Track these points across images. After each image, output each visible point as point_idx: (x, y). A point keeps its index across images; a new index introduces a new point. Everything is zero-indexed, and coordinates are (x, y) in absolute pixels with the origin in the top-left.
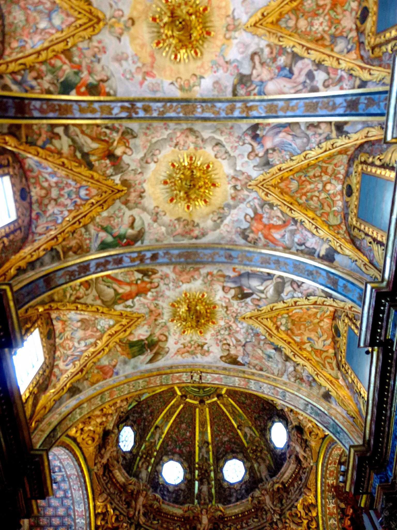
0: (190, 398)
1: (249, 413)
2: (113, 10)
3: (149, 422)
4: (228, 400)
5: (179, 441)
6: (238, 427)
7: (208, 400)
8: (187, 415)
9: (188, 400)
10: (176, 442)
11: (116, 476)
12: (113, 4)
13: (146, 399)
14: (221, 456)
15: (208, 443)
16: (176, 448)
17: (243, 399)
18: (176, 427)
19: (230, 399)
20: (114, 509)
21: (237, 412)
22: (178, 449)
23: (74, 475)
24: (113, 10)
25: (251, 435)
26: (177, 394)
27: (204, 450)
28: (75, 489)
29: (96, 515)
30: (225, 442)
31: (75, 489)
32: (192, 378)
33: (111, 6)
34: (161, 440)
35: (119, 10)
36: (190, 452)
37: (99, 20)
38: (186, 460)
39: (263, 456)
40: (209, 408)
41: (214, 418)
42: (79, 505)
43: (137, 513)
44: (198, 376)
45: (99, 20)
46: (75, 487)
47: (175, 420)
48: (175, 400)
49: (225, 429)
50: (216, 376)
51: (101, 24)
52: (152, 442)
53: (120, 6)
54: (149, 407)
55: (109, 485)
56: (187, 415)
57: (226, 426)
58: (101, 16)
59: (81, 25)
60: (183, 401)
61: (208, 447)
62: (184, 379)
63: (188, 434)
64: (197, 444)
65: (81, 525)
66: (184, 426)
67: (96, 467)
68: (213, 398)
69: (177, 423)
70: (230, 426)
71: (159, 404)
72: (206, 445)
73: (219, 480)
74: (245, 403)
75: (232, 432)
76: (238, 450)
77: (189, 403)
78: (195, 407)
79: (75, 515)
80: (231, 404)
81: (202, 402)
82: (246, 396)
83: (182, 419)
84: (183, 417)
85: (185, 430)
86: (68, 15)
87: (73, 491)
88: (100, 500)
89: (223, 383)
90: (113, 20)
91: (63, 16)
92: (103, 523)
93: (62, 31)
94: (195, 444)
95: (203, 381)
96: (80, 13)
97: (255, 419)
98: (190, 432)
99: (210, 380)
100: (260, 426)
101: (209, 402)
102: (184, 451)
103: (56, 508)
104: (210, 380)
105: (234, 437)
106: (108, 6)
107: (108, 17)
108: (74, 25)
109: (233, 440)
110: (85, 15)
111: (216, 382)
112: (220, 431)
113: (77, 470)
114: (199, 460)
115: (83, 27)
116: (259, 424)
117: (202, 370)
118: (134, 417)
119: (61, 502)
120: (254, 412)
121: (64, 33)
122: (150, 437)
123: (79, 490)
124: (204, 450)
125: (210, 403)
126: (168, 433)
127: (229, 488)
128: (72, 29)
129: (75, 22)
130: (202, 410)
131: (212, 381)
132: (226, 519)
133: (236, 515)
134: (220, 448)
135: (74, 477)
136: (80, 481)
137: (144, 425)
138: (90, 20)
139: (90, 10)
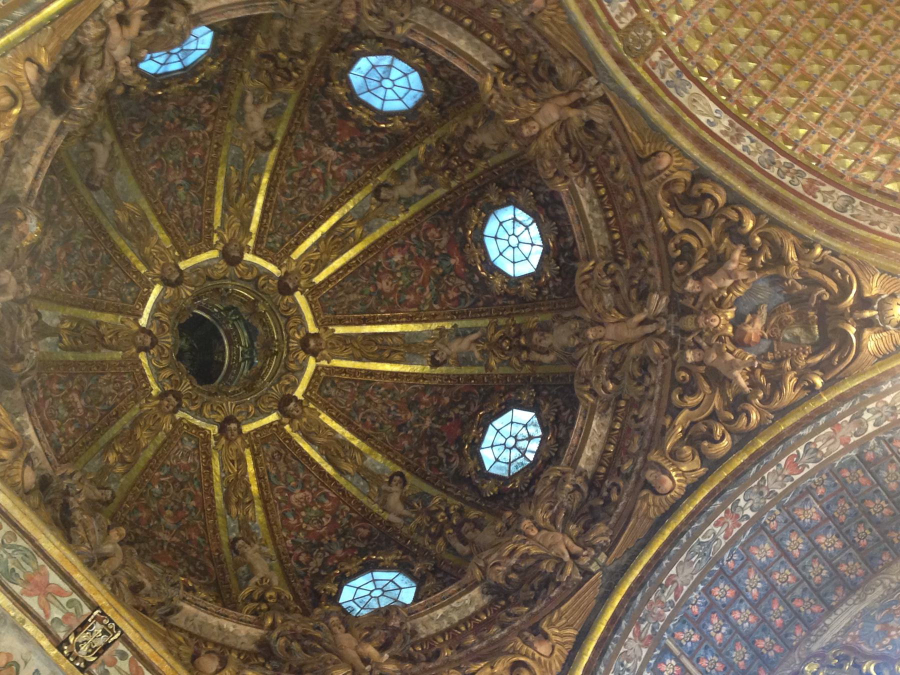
0: (303, 324)
1: (204, 150)
3: (438, 395)
4: (222, 227)
5: (434, 274)
6: (270, 148)
7: (270, 274)
8: (353, 297)
9: (312, 329)
10: (439, 279)
11: (597, 452)
13: (384, 450)
14: (380, 135)
15: (376, 192)
16: (453, 268)
17: (181, 192)
18: (404, 303)
19: (217, 224)
20: (674, 411)
21: (234, 177)
22: (453, 261)
23: (638, 635)
25: (257, 103)
26: (316, 370)
27: (403, 190)
28: (678, 590)
29: (713, 465)
30: (338, 149)
31: (678, 590)
32: (106, 646)
34: (463, 324)
36: (437, 224)
38: (462, 220)
39: (275, 43)
40: (288, 255)
41: (305, 221)
42: (709, 544)
43: (649, 329)
44: (83, 636)
46: (672, 597)
47: (386, 321)
48: (336, 363)
49: (306, 174)
50: (33, 602)
52: (482, 352)
54: (401, 426)
55: (626, 467)
56: (353, 297)
57: (297, 175)
60: (325, 337)
61: (386, 185)
62: (124, 665)
63: (397, 258)
64: (402, 217)
65: (755, 498)
66: (385, 285)
67: (594, 567)
68: (251, 266)
69: (392, 308)
70: (289, 165)
71: (376, 399)
72: (383, 194)
73: (441, 108)
74: (188, 179)
75: (297, 151)
76: (330, 104)
77: (315, 319)
78: (313, 292)
79: (742, 531)
80: (225, 209)
81: (285, 287)
82: (164, 195)
83: (372, 301)
84: (364, 302)
85: (393, 273)
87: (685, 588)
88: (668, 484)
89: (41, 562)
92: (719, 430)
94: (406, 223)
95: (86, 610)
97: (204, 124)
98: (387, 258)
99: (64, 601)
100: (210, 101)
101: (272, 268)
102: (445, 241)
103: (764, 570)
104: (64, 601)
105: (307, 136)
109: (315, 133)
111: (54, 579)
112: (323, 180)
113: (621, 643)
114: (436, 186)
116: (207, 107)
117: (54, 652)
118: (449, 456)
119: (741, 574)
120: (188, 141)
122: (472, 364)
123: (672, 581)
124: (403, 190)
125: (272, 262)
126: (432, 319)
127: (436, 74)
130: (307, 269)
131: (61, 593)
132: (507, 53)
133: (473, 32)
134: (365, 154)
135: (646, 628)
136: (646, 600)
137: (453, 405)
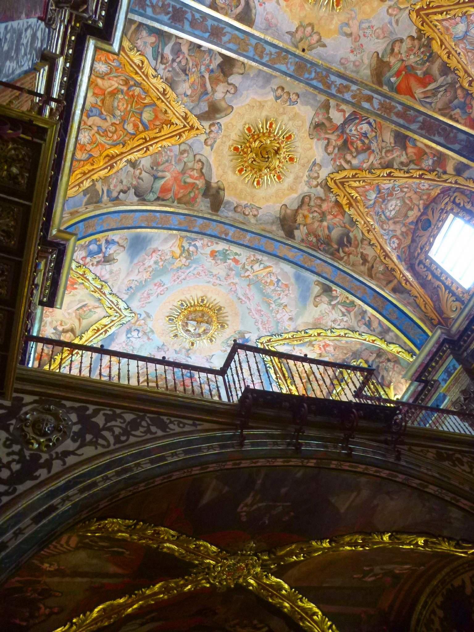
2: (397, 17)
12: (394, 24)
24: (397, 17)
33: (397, 22)
35: (391, 15)
37: (418, 12)
45: (418, 12)
51: (418, 7)
53: (387, 18)
58: (414, 15)
59: (441, 13)
86: (447, 29)
90: (402, 7)
91: (452, 30)
93: (464, 14)
96: (436, 26)
106: (400, 24)
107: (407, 11)
108: (449, 16)
110: (431, 22)
115: (439, 10)
121: (465, 10)
128: (453, 13)
129: (443, 20)
138: (427, 15)
139: (422, 25)
